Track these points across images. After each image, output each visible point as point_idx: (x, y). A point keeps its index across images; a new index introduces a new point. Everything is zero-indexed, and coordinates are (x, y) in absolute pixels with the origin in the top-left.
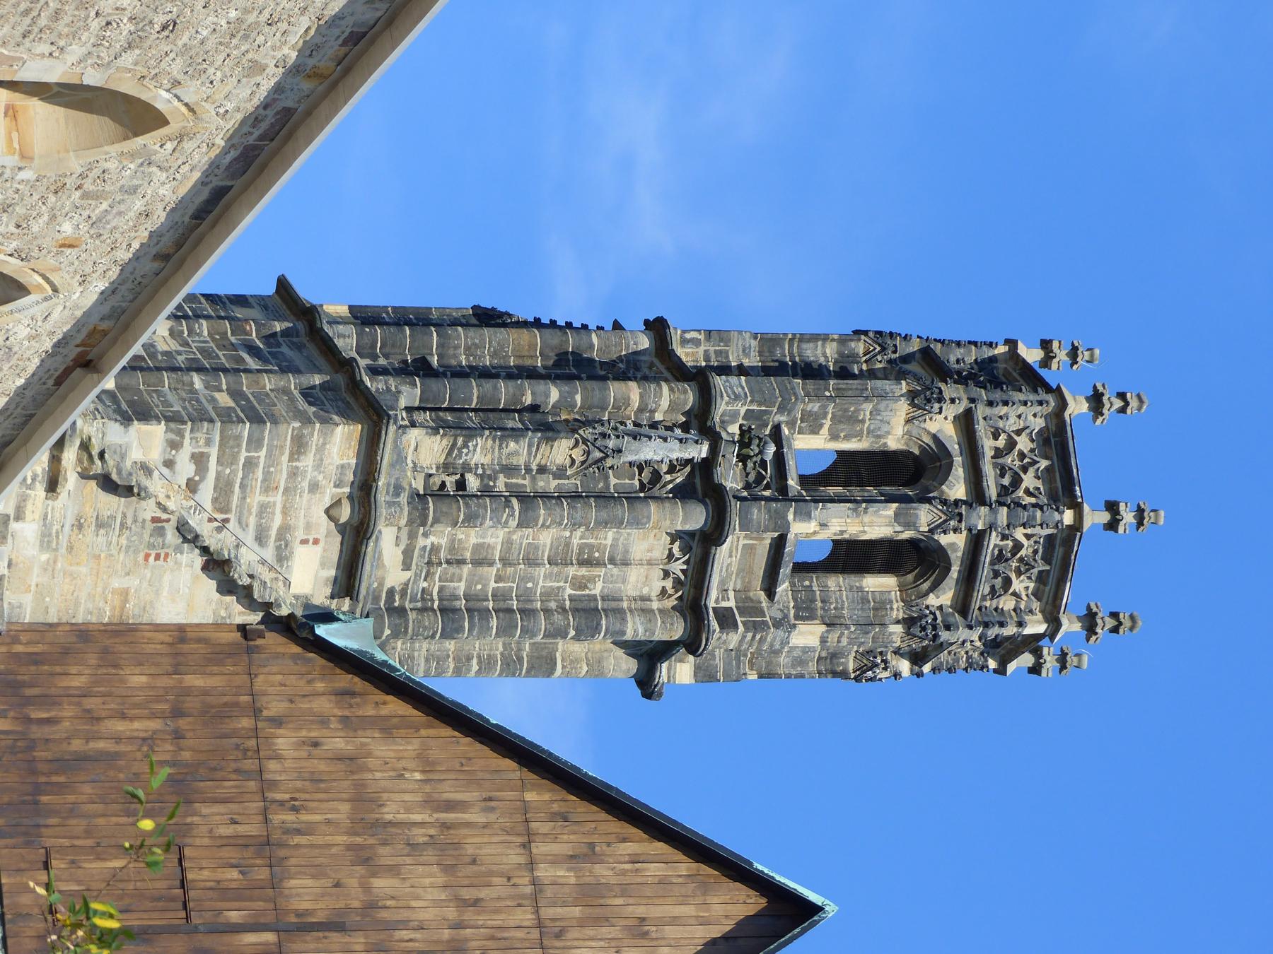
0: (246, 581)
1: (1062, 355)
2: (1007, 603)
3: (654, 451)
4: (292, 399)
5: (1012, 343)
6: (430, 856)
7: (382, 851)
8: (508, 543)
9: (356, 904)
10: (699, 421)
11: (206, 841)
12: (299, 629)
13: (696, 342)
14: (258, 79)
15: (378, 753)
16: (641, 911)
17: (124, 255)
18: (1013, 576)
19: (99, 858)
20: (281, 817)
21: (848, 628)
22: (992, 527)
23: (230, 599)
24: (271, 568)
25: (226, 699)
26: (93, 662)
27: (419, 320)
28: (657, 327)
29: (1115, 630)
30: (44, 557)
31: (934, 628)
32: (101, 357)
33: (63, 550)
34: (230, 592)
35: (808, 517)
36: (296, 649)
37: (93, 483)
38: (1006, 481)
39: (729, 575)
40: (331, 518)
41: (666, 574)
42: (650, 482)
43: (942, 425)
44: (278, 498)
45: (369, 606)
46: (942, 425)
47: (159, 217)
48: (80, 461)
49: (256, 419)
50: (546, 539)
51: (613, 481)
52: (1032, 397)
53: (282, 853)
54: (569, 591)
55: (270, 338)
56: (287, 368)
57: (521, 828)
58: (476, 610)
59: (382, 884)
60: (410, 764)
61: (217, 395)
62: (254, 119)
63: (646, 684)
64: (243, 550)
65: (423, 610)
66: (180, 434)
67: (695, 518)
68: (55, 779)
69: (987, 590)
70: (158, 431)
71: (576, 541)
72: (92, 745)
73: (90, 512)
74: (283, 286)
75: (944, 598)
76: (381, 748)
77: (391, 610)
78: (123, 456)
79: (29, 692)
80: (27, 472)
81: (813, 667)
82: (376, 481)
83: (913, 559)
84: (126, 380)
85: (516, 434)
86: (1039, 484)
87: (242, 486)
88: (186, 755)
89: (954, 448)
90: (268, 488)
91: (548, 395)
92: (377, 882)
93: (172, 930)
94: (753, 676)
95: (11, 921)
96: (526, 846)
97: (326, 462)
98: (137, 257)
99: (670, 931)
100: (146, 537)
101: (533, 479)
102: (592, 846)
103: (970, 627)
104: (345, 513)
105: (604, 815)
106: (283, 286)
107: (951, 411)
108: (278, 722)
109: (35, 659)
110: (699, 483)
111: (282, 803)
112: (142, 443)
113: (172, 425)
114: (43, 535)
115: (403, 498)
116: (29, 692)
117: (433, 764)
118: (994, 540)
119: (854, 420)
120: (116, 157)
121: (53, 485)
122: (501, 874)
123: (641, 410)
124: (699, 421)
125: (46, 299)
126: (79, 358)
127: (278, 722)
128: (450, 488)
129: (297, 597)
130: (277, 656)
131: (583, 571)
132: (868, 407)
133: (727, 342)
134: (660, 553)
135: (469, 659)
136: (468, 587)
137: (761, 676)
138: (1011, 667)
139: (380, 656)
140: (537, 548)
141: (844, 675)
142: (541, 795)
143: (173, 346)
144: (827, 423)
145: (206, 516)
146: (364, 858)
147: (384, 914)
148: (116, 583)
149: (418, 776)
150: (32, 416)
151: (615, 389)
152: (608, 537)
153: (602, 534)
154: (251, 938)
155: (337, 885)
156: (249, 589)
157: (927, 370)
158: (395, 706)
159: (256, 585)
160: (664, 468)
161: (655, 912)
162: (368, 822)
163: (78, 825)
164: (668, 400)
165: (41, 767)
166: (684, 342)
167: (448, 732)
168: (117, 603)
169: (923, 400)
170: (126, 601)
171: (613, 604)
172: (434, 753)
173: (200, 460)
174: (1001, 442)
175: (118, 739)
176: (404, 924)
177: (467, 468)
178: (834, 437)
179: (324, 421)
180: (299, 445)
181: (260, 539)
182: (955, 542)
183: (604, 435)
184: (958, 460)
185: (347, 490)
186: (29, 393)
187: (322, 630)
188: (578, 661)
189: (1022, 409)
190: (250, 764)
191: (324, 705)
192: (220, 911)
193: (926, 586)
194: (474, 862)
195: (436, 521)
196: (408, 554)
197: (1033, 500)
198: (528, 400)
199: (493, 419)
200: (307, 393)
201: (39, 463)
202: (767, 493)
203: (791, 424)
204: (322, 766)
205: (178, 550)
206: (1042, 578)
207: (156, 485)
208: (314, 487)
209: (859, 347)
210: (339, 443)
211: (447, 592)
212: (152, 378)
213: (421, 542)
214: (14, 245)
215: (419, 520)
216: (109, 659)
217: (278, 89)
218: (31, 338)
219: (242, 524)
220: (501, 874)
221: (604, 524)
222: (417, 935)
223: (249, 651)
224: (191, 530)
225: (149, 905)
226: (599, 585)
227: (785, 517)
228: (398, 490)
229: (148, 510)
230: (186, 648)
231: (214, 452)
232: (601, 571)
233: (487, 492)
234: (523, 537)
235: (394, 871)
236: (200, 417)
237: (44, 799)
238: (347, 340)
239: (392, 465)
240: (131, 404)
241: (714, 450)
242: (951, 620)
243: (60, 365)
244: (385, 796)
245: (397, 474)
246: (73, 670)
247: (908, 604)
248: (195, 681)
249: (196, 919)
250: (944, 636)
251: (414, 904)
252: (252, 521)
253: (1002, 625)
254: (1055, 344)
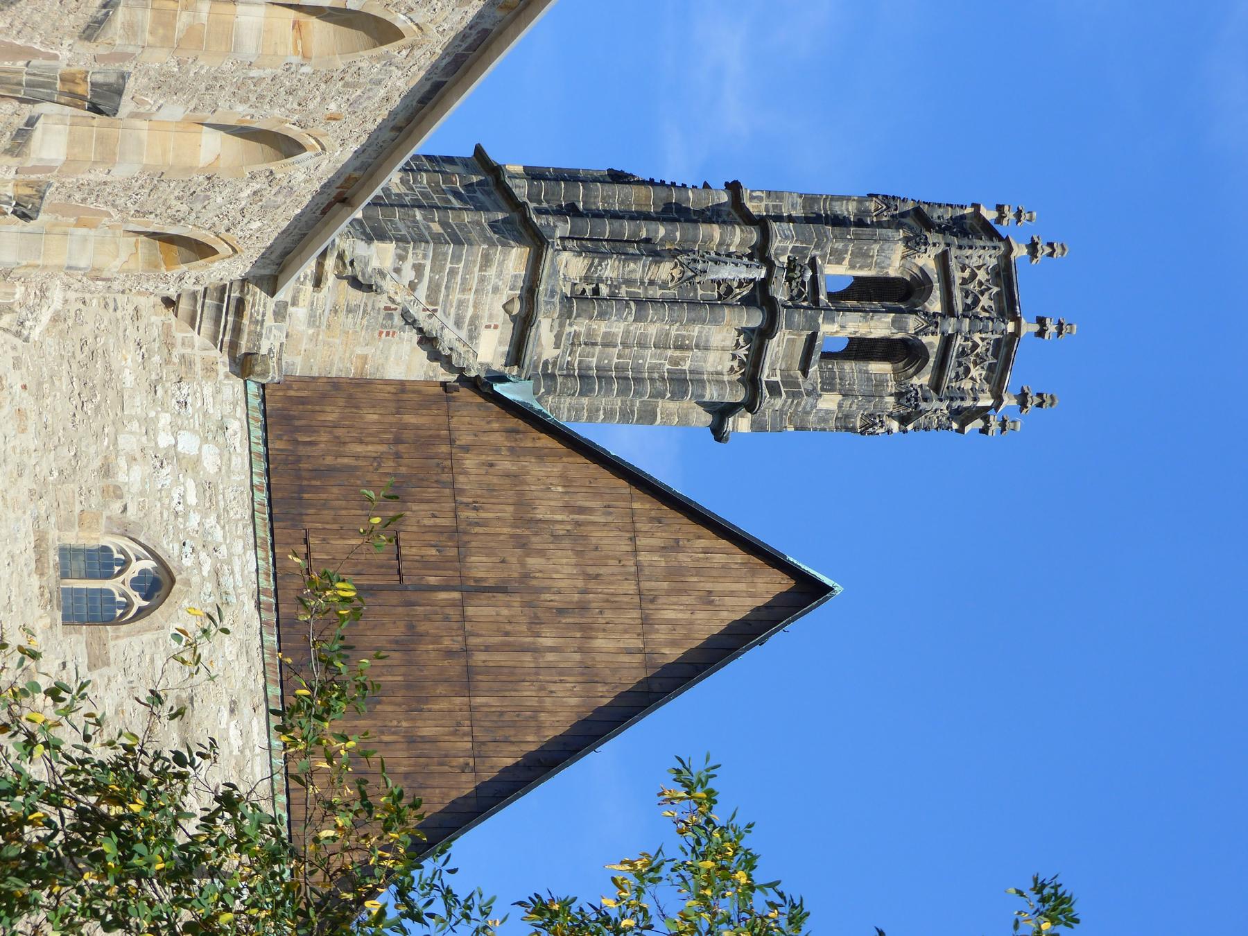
0: (447, 352)
1: (1010, 215)
2: (967, 385)
3: (728, 272)
4: (482, 229)
5: (976, 206)
6: (566, 543)
7: (534, 539)
8: (627, 332)
9: (515, 575)
10: (760, 253)
11: (415, 529)
12: (482, 386)
13: (760, 199)
14: (467, 8)
15: (533, 473)
16: (709, 586)
17: (371, 127)
18: (971, 366)
19: (342, 538)
20: (465, 514)
21: (857, 397)
22: (958, 332)
23: (437, 364)
24: (465, 344)
25: (431, 432)
26: (341, 404)
27: (571, 177)
28: (734, 188)
29: (1040, 405)
30: (310, 332)
31: (916, 400)
32: (353, 196)
33: (324, 327)
34: (436, 360)
35: (833, 321)
36: (481, 400)
37: (345, 282)
38: (969, 301)
39: (777, 359)
40: (506, 311)
41: (734, 357)
42: (725, 295)
43: (927, 261)
44: (471, 297)
45: (531, 372)
46: (927, 261)
47: (396, 101)
48: (337, 267)
49: (458, 242)
50: (652, 330)
51: (700, 292)
52: (989, 244)
53: (466, 538)
54: (667, 366)
55: (468, 187)
56: (479, 208)
57: (629, 527)
58: (603, 377)
59: (533, 562)
60: (555, 481)
61: (432, 225)
62: (463, 36)
63: (718, 432)
64: (446, 331)
65: (567, 376)
66: (406, 250)
67: (755, 319)
68: (314, 483)
69: (953, 375)
70: (390, 248)
71: (673, 333)
72: (340, 460)
73: (343, 302)
74: (479, 151)
75: (923, 380)
76: (536, 470)
77: (545, 375)
78: (366, 264)
79: (297, 423)
80: (301, 273)
81: (832, 424)
82: (538, 287)
83: (903, 352)
84: (370, 213)
85: (635, 258)
86: (992, 303)
87: (447, 288)
88: (403, 470)
89: (934, 277)
90: (464, 290)
91: (657, 232)
92: (530, 561)
93: (391, 588)
94: (791, 429)
95: (281, 578)
96: (632, 539)
97: (505, 272)
98: (380, 128)
99: (729, 601)
100: (380, 320)
101: (646, 289)
102: (677, 541)
103: (941, 400)
104: (516, 308)
105: (686, 520)
106: (479, 151)
107: (933, 252)
108: (466, 449)
109: (302, 401)
110: (759, 296)
111: (467, 504)
112: (380, 255)
113: (400, 244)
114: (311, 316)
115: (557, 299)
116: (297, 423)
117: (571, 481)
118: (959, 341)
119: (866, 255)
120: (368, 59)
121: (318, 283)
122: (614, 558)
123: (720, 244)
124: (760, 253)
125: (317, 155)
126: (338, 196)
127: (466, 449)
128: (589, 294)
129: (481, 364)
130: (467, 404)
131: (678, 353)
132: (876, 247)
133: (781, 199)
134: (730, 342)
135: (598, 410)
136: (599, 361)
137: (796, 429)
138: (968, 428)
139: (537, 406)
140: (646, 336)
141: (853, 430)
142: (643, 505)
143: (403, 190)
144: (848, 257)
145: (421, 307)
146: (522, 544)
147: (534, 583)
148: (359, 351)
149: (560, 489)
150: (305, 235)
151: (703, 229)
152: (695, 330)
153: (691, 328)
154: (443, 595)
155: (503, 561)
156: (449, 357)
157: (917, 222)
158: (546, 441)
159: (454, 356)
160: (735, 284)
161: (719, 587)
162: (525, 519)
163: (328, 514)
164: (739, 237)
165: (304, 474)
166: (752, 198)
167: (582, 460)
168: (359, 364)
169: (914, 243)
170: (365, 363)
171: (697, 377)
172: (572, 474)
173: (418, 268)
174: (967, 274)
175: (357, 457)
176: (547, 590)
177: (600, 280)
178: (852, 266)
179: (504, 245)
180: (487, 261)
181: (458, 324)
182: (932, 341)
183: (695, 261)
184: (936, 285)
185: (518, 292)
186: (304, 219)
187: (497, 388)
188: (672, 414)
189: (982, 252)
190: (446, 477)
191: (498, 438)
192: (423, 577)
193: (911, 371)
194: (596, 549)
195: (578, 315)
196: (558, 337)
197: (987, 315)
198: (644, 234)
199: (619, 247)
200: (493, 225)
201: (309, 267)
202: (805, 304)
203: (823, 257)
204: (495, 480)
205: (402, 329)
206: (991, 368)
207: (388, 285)
208: (496, 290)
209: (872, 206)
210: (515, 259)
211: (584, 365)
212: (388, 211)
213: (568, 329)
214: (296, 117)
215: (566, 314)
216: (353, 402)
217: (480, 15)
218: (306, 181)
219: (447, 314)
220: (614, 558)
221: (692, 321)
222: (556, 597)
223: (448, 400)
224: (411, 316)
225: (374, 570)
226: (688, 363)
227: (816, 321)
228: (553, 293)
229: (382, 301)
230: (405, 396)
231: (428, 263)
232: (690, 354)
233: (613, 297)
234: (638, 329)
235: (541, 553)
236: (420, 239)
237: (306, 496)
238: (521, 190)
239: (549, 276)
240: (372, 228)
241: (770, 273)
242: (928, 395)
243: (325, 200)
244: (537, 502)
245: (552, 282)
246: (328, 409)
247: (899, 383)
248: (410, 419)
249: (406, 581)
250: (923, 405)
251: (555, 576)
252: (453, 311)
253: (962, 399)
254: (1006, 208)
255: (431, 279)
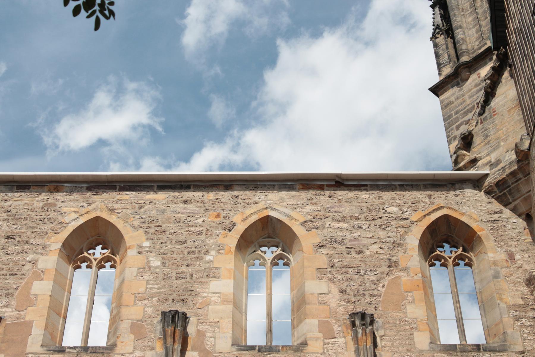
44: (466, 97)
87: (465, 108)
231: (454, 126)
255: (462, 119)
